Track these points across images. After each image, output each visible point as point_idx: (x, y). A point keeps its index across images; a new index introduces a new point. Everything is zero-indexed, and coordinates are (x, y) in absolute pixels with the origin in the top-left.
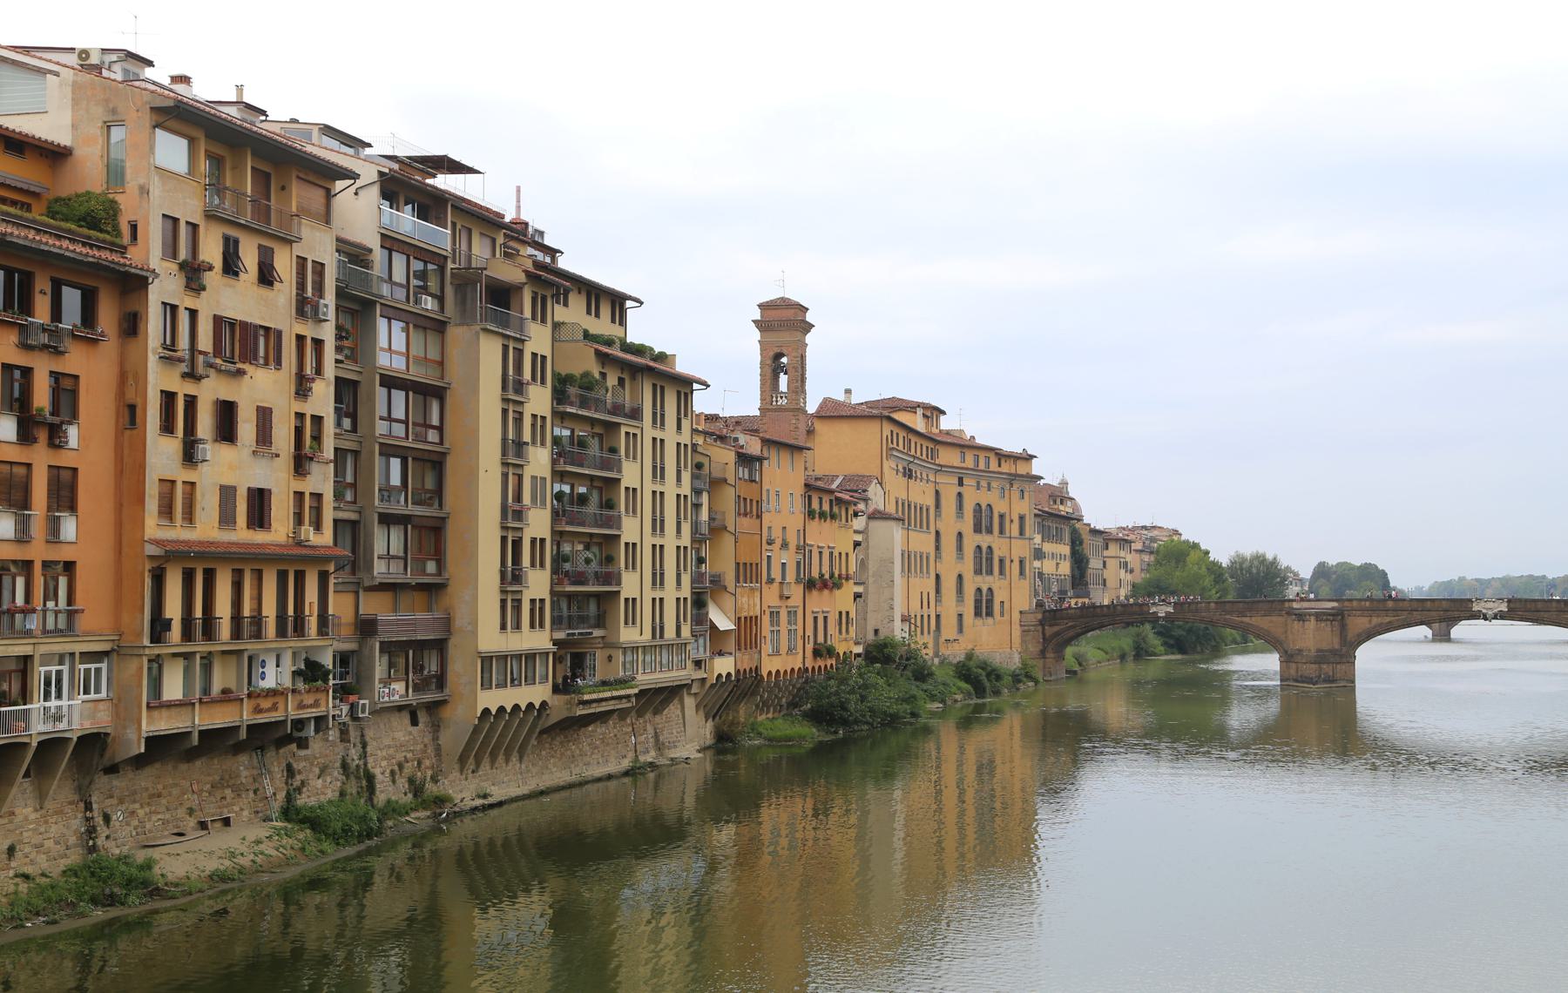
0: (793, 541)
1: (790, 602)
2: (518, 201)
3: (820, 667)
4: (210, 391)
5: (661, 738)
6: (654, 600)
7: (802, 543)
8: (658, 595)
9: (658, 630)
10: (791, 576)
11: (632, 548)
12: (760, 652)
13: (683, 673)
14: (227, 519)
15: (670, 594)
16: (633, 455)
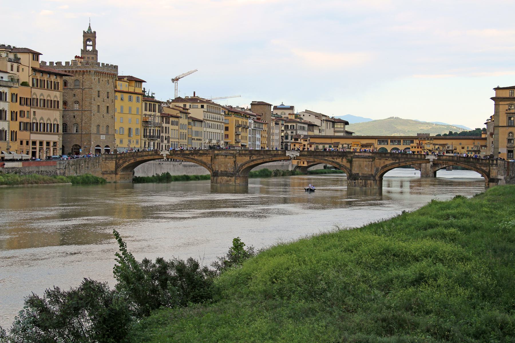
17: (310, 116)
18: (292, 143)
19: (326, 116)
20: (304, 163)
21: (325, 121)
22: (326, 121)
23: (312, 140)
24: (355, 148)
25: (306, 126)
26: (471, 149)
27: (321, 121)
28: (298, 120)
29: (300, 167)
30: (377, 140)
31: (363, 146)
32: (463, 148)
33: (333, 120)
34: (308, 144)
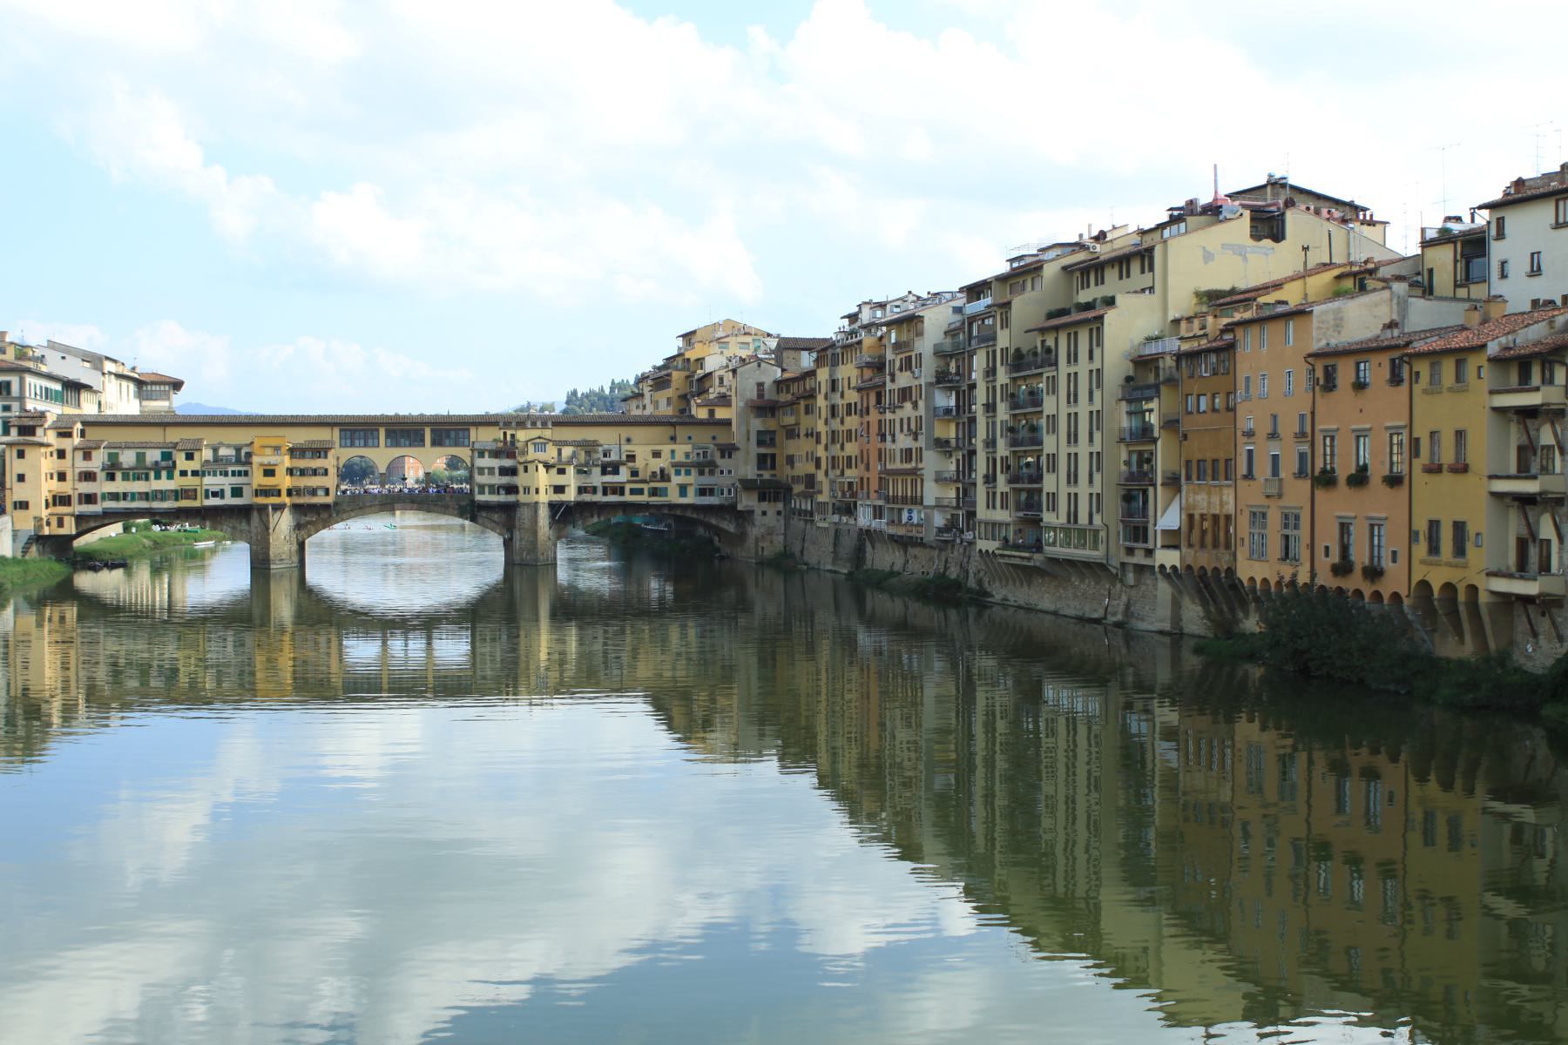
0: (1289, 427)
1: (1285, 502)
2: (1216, 176)
3: (1358, 593)
4: (900, 414)
5: (1132, 609)
6: (1069, 494)
7: (1308, 429)
8: (1072, 490)
9: (1073, 516)
10: (1289, 466)
11: (1053, 458)
12: (1235, 555)
13: (1095, 553)
14: (902, 461)
15: (1083, 489)
16: (1054, 390)
17: (63, 358)
18: (10, 445)
19: (115, 361)
20: (61, 524)
21: (113, 376)
22: (120, 376)
23: (93, 434)
24: (266, 460)
25: (58, 387)
26: (683, 459)
27: (104, 374)
28: (31, 365)
29: (50, 537)
30: (336, 431)
31: (295, 452)
32: (657, 454)
33: (136, 376)
34: (75, 449)
